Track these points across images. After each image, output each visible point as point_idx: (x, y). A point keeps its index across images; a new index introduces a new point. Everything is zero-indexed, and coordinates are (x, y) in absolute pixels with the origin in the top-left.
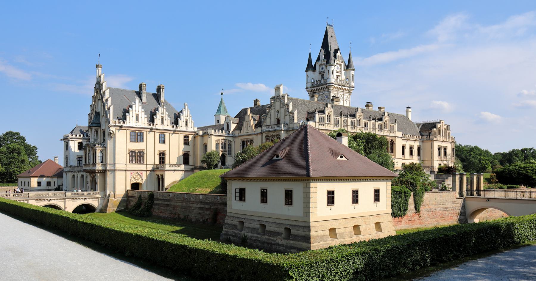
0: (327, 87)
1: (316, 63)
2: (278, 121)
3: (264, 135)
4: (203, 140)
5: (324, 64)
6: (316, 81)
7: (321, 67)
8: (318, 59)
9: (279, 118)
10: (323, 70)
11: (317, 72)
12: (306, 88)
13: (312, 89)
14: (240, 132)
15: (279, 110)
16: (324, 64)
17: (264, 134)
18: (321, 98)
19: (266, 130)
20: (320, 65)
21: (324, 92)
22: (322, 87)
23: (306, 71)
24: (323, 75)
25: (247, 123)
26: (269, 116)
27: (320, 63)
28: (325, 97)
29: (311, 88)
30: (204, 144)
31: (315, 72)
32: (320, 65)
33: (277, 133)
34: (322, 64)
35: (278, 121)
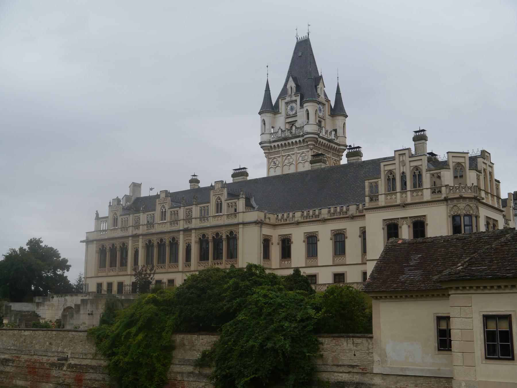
0: (303, 140)
1: (280, 100)
5: (296, 101)
6: (282, 130)
7: (289, 106)
8: (284, 93)
10: (294, 112)
12: (260, 144)
13: (272, 145)
16: (296, 101)
18: (291, 160)
20: (287, 103)
21: (296, 151)
22: (294, 141)
23: (260, 113)
28: (301, 159)
29: (270, 142)
31: (279, 115)
34: (292, 102)
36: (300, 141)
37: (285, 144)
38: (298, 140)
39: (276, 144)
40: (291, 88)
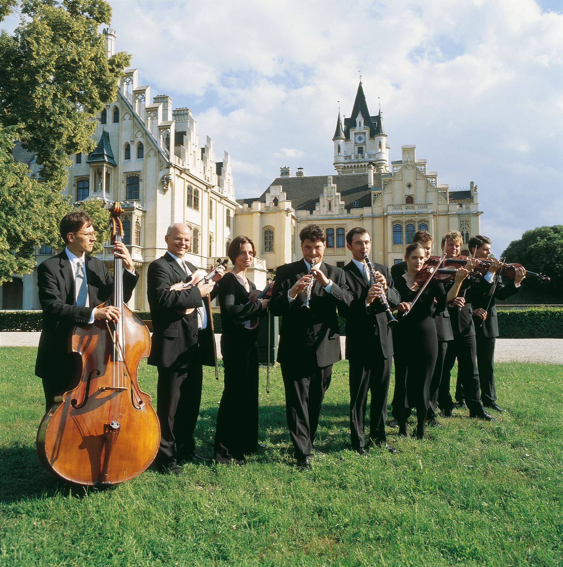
2: (410, 200)
4: (262, 221)
5: (365, 133)
9: (413, 195)
10: (362, 141)
11: (350, 142)
13: (346, 165)
14: (311, 213)
16: (365, 133)
17: (389, 217)
20: (355, 134)
26: (388, 190)
27: (357, 129)
29: (344, 163)
30: (263, 229)
32: (355, 134)
33: (423, 218)
34: (360, 133)
35: (410, 200)
37: (358, 166)
39: (350, 165)
40: (360, 122)
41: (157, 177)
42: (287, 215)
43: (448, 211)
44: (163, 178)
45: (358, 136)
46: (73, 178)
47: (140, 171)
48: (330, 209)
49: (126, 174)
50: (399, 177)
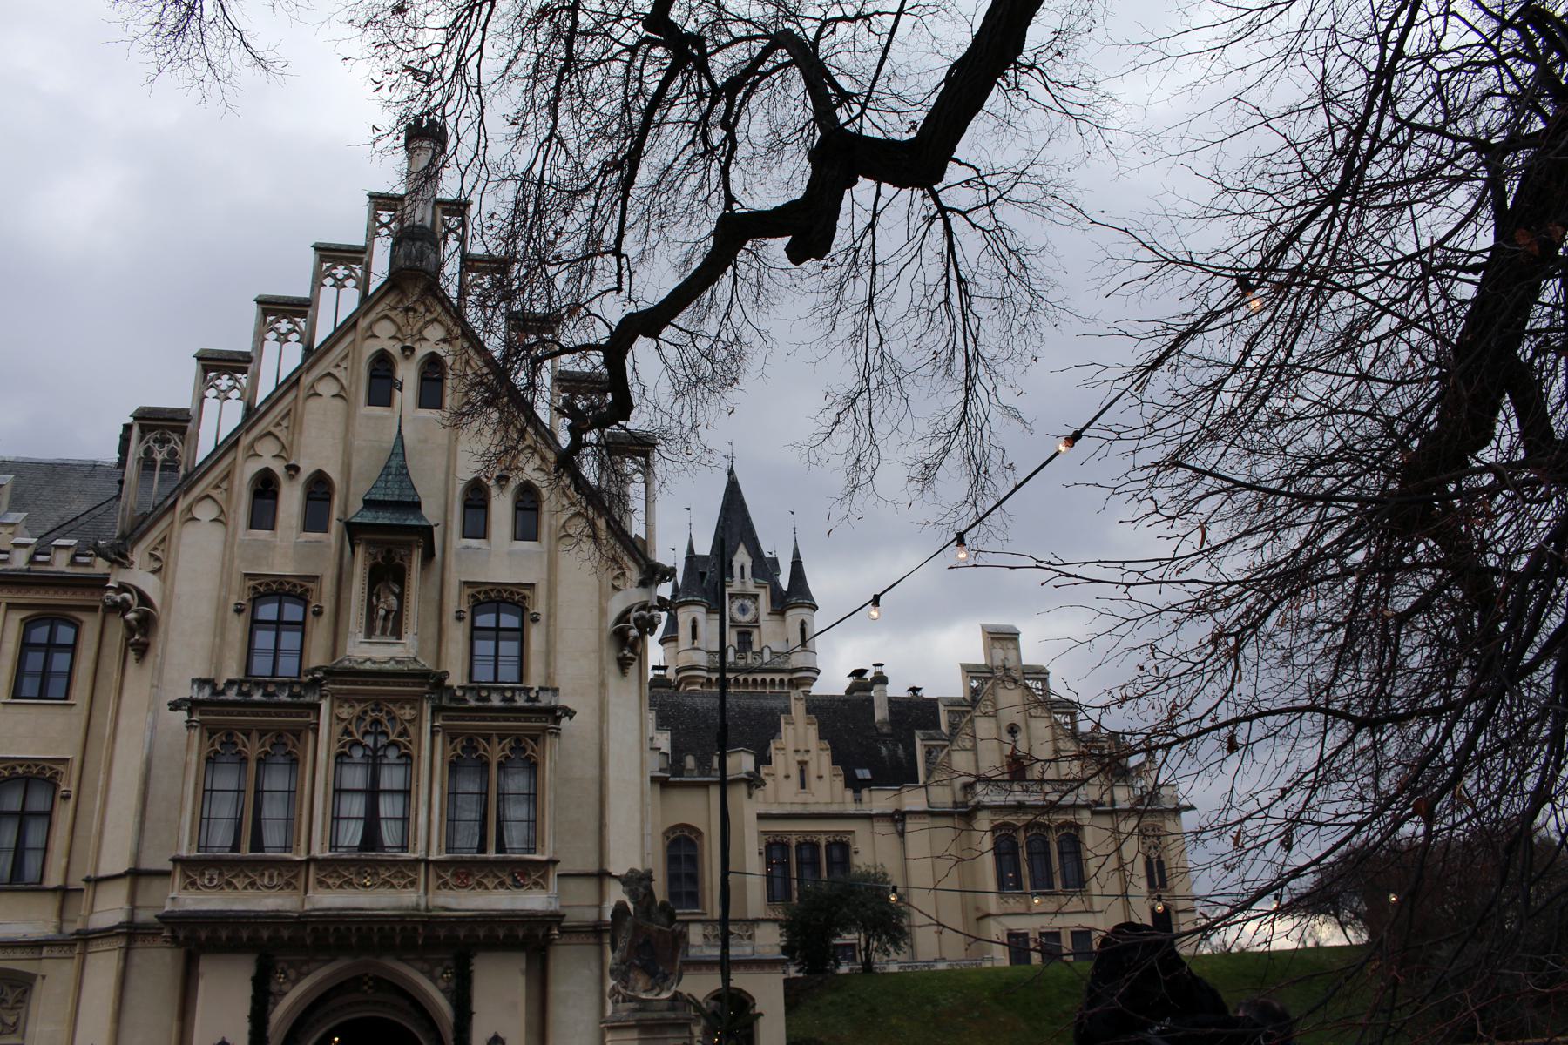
0: (790, 680)
3: (984, 822)
5: (755, 597)
10: (748, 617)
15: (1021, 724)
16: (755, 597)
19: (994, 798)
22: (768, 677)
24: (750, 634)
25: (799, 758)
32: (731, 596)
34: (743, 596)
35: (1017, 767)
36: (782, 681)
37: (746, 680)
38: (777, 677)
40: (742, 568)
41: (603, 612)
42: (750, 796)
43: (1113, 802)
44: (624, 616)
45: (737, 604)
46: (236, 581)
47: (531, 586)
48: (803, 786)
49: (470, 591)
50: (986, 706)
